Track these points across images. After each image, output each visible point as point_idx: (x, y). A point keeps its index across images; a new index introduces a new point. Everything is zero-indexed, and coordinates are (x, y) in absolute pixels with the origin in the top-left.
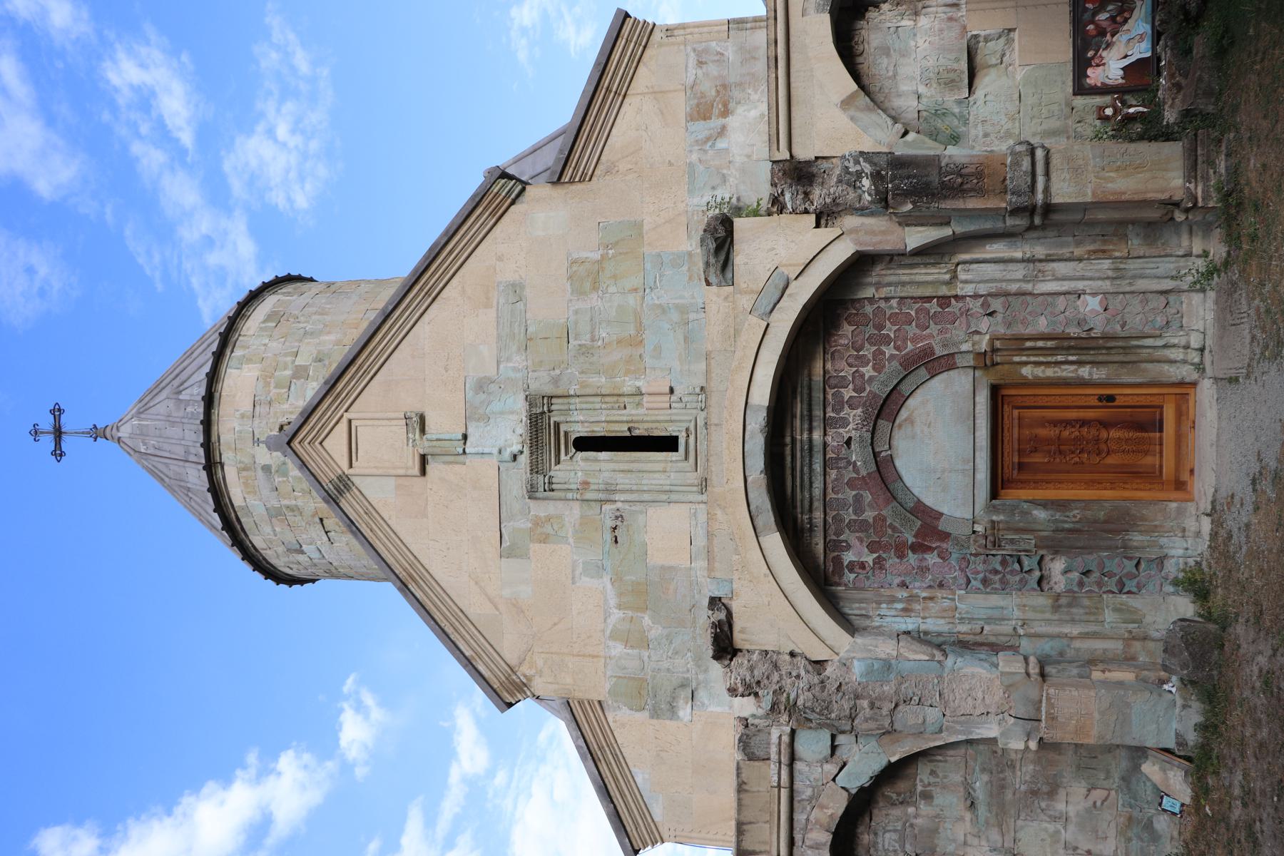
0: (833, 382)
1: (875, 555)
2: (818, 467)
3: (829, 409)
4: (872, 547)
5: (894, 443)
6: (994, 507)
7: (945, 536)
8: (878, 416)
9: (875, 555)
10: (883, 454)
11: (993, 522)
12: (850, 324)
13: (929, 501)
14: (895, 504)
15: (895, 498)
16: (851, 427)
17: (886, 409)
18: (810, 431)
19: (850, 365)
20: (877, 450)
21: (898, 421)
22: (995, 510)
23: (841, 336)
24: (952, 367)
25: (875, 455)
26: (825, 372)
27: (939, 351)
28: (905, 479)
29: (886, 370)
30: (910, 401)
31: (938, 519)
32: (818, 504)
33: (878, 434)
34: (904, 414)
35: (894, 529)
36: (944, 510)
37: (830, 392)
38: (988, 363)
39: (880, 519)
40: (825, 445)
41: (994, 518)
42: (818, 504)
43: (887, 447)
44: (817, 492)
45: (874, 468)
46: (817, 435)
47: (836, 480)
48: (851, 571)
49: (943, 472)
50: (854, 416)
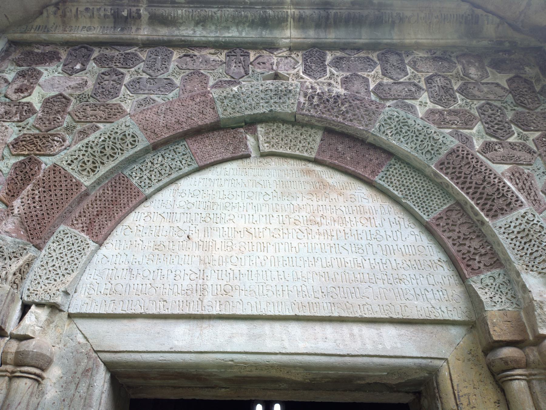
0: (393, 59)
1: (37, 106)
2: (233, 34)
3: (339, 54)
4: (56, 104)
5: (274, 162)
6: (88, 372)
7: (36, 231)
8: (330, 132)
9: (37, 106)
10: (251, 140)
11: (43, 363)
12: (510, 81)
13: (137, 219)
14: (143, 143)
15: (155, 147)
16: (309, 80)
17: (347, 147)
18: (301, 22)
19: (429, 80)
20: (260, 129)
21: (318, 169)
22: (79, 375)
23: (482, 68)
24: (461, 266)
25: (251, 123)
26: (408, 49)
27: (499, 227)
28: (197, 178)
29: (434, 128)
30: (361, 192)
31: (88, 229)
32: (163, 33)
33: (291, 132)
34: (336, 179)
35: (84, 133)
36: (110, 248)
37: (374, 56)
38: (507, 352)
39: (114, 113)
40: (271, 47)
41: (54, 374)
42: (163, 33)
43: (265, 148)
44: (187, 32)
45: (224, 113)
46: (289, 34)
47: (207, 61)
48: (22, 75)
49: (205, 246)
50: (333, 82)
